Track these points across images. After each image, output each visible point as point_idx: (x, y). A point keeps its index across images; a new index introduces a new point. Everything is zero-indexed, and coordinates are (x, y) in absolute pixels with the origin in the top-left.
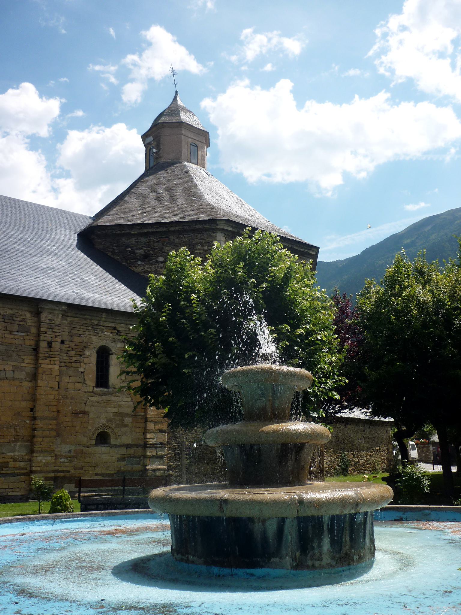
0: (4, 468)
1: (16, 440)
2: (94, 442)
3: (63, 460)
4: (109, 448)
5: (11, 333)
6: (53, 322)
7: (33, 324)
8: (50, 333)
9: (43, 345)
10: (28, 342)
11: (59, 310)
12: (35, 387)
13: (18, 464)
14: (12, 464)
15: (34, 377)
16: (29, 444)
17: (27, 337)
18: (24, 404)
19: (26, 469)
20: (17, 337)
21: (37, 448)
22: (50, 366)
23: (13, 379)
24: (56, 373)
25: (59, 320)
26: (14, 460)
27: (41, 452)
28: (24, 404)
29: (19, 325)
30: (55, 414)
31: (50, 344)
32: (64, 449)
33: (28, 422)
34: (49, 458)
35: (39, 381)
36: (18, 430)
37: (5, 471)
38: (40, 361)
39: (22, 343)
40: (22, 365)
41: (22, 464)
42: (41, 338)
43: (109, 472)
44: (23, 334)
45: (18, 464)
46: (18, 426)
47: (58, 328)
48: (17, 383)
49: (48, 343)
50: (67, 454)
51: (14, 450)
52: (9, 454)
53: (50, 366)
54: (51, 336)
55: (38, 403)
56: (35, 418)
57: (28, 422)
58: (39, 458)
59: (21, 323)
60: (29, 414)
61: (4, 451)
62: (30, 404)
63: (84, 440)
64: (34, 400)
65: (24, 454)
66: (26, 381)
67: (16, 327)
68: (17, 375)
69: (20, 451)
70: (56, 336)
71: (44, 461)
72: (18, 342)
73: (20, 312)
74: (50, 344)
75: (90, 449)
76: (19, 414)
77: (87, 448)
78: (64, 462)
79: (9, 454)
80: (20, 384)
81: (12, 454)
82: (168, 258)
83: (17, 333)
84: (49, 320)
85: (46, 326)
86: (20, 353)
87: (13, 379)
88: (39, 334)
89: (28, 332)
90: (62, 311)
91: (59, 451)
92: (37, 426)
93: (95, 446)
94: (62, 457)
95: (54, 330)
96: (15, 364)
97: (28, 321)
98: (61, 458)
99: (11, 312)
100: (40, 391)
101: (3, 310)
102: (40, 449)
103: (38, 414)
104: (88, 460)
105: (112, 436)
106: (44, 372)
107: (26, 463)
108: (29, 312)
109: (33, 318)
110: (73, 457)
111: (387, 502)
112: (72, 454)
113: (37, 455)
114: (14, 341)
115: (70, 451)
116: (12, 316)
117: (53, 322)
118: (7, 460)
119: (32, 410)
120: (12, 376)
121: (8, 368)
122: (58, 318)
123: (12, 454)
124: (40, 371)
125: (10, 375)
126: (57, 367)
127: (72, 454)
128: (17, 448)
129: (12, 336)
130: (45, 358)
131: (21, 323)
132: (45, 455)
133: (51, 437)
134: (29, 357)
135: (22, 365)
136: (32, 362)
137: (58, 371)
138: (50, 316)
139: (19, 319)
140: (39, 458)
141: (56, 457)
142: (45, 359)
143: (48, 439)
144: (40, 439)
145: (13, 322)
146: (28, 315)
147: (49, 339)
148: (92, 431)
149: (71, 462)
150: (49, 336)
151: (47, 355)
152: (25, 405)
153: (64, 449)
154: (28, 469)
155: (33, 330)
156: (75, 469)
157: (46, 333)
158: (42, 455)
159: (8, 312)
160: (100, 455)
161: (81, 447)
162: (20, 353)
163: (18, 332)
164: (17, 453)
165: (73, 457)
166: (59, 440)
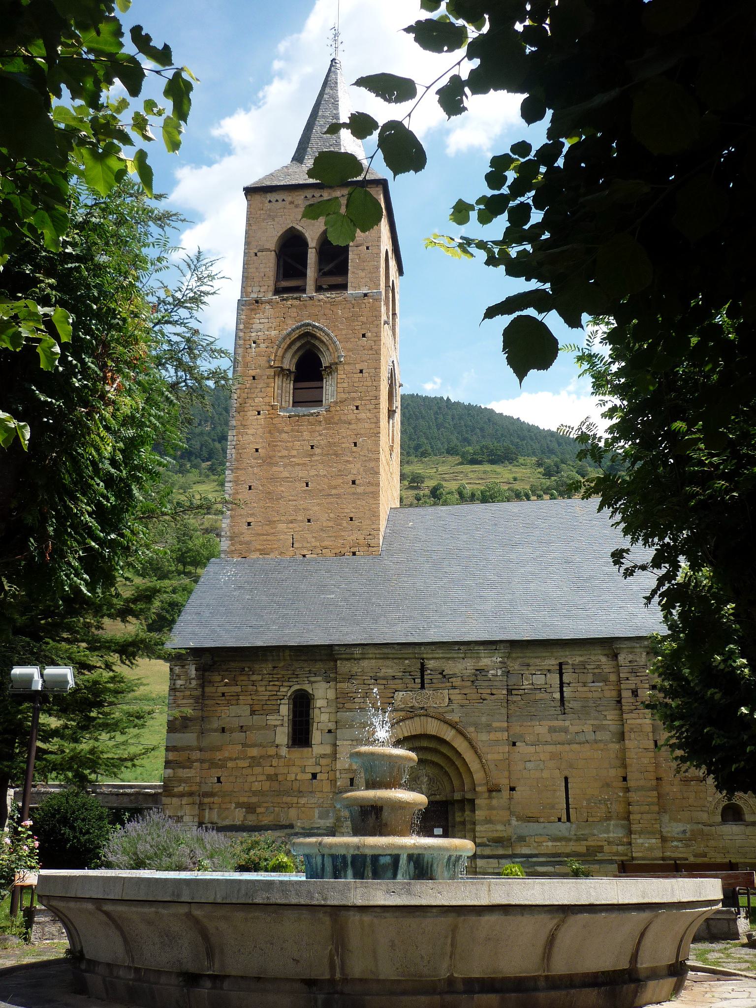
0: (598, 854)
1: (608, 818)
2: (719, 818)
3: (675, 843)
4: (743, 827)
5: (585, 684)
6: (635, 664)
7: (612, 670)
8: (633, 678)
9: (626, 694)
10: (608, 694)
11: (641, 647)
12: (624, 750)
13: (615, 848)
14: (606, 848)
15: (621, 737)
16: (626, 822)
17: (607, 687)
18: (613, 772)
19: (626, 855)
20: (593, 689)
21: (635, 827)
22: (639, 721)
23: (596, 742)
24: (649, 729)
25: (643, 660)
26: (609, 843)
27: (641, 833)
28: (613, 772)
29: (594, 674)
30: (654, 783)
31: (635, 693)
32: (674, 828)
33: (621, 794)
34: (654, 841)
35: (627, 742)
36: (609, 806)
37: (600, 856)
38: (625, 716)
39: (600, 695)
40: (605, 722)
41: (620, 848)
42: (623, 686)
43: (747, 861)
44: (601, 684)
45: (615, 848)
46: (609, 800)
47: (643, 670)
48: (602, 746)
49: (633, 692)
50: (681, 836)
51: (607, 831)
52: (601, 836)
53: (639, 721)
54: (635, 682)
55: (629, 769)
56: (627, 790)
57: (621, 794)
58: (640, 841)
59: (596, 671)
60: (622, 784)
61: (595, 832)
62: (620, 772)
63: (704, 817)
64: (624, 766)
65: (620, 835)
66: (613, 742)
67: (590, 677)
68: (599, 736)
69: (616, 833)
70: (641, 681)
71: (647, 845)
72: (596, 695)
73: (593, 658)
74: (635, 693)
75: (713, 828)
76: (608, 785)
77: (709, 828)
78: (677, 847)
79: (601, 836)
80: (605, 747)
81: (606, 835)
82: (702, 571)
83: (593, 684)
84: (630, 662)
85: (626, 670)
86: (601, 708)
87: (596, 742)
88: (619, 681)
89: (605, 681)
90: (645, 647)
91: (668, 832)
92: (631, 800)
93: (721, 825)
94: (674, 839)
95: (638, 674)
96: (596, 722)
97: (603, 667)
98: (672, 841)
99: (581, 659)
100: (631, 755)
101: (571, 658)
102: (639, 829)
103: (631, 783)
104: (712, 843)
105: (746, 810)
106: (632, 729)
107: (626, 847)
108: (605, 655)
109: (611, 662)
110: (690, 840)
111: (528, 868)
112: (688, 835)
113: (637, 836)
114: (590, 695)
115: (684, 832)
116: (583, 665)
117: (635, 664)
118: (600, 843)
119: (625, 779)
120: (593, 737)
121: (588, 728)
122: (641, 657)
123: (606, 835)
124: (626, 729)
125: (591, 737)
126: (648, 721)
127: (688, 835)
128: (611, 828)
129: (586, 689)
130: (631, 711)
131: (596, 671)
132: (647, 836)
133: (653, 813)
134: (613, 712)
135: (605, 722)
136: (616, 717)
137: (651, 726)
138: (630, 657)
139: (592, 667)
140: (640, 841)
141: (664, 839)
142: (632, 712)
143: (649, 816)
144: (638, 817)
145: (586, 671)
146: (604, 659)
147: (633, 687)
148: (714, 803)
149: (687, 846)
150: (632, 683)
151: (634, 707)
152: (614, 773)
153: (674, 828)
154: (630, 855)
155: (613, 678)
156: (695, 856)
157: (628, 679)
158: (642, 836)
159: (578, 659)
160: (730, 837)
161: (700, 826)
162: (601, 708)
163: (593, 682)
164: (611, 835)
165: (690, 840)
166: (666, 818)
